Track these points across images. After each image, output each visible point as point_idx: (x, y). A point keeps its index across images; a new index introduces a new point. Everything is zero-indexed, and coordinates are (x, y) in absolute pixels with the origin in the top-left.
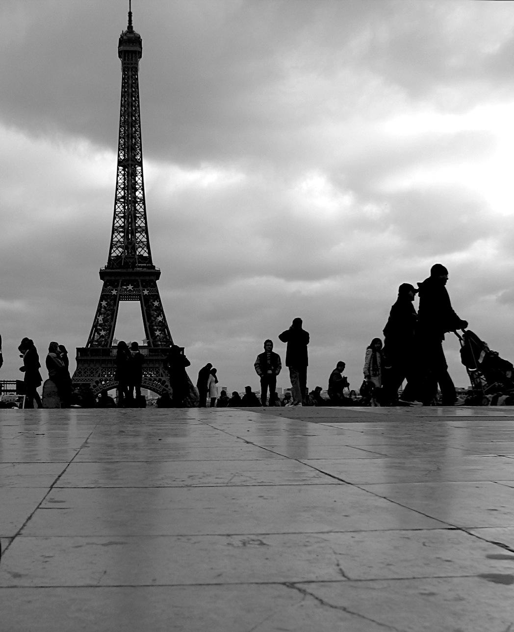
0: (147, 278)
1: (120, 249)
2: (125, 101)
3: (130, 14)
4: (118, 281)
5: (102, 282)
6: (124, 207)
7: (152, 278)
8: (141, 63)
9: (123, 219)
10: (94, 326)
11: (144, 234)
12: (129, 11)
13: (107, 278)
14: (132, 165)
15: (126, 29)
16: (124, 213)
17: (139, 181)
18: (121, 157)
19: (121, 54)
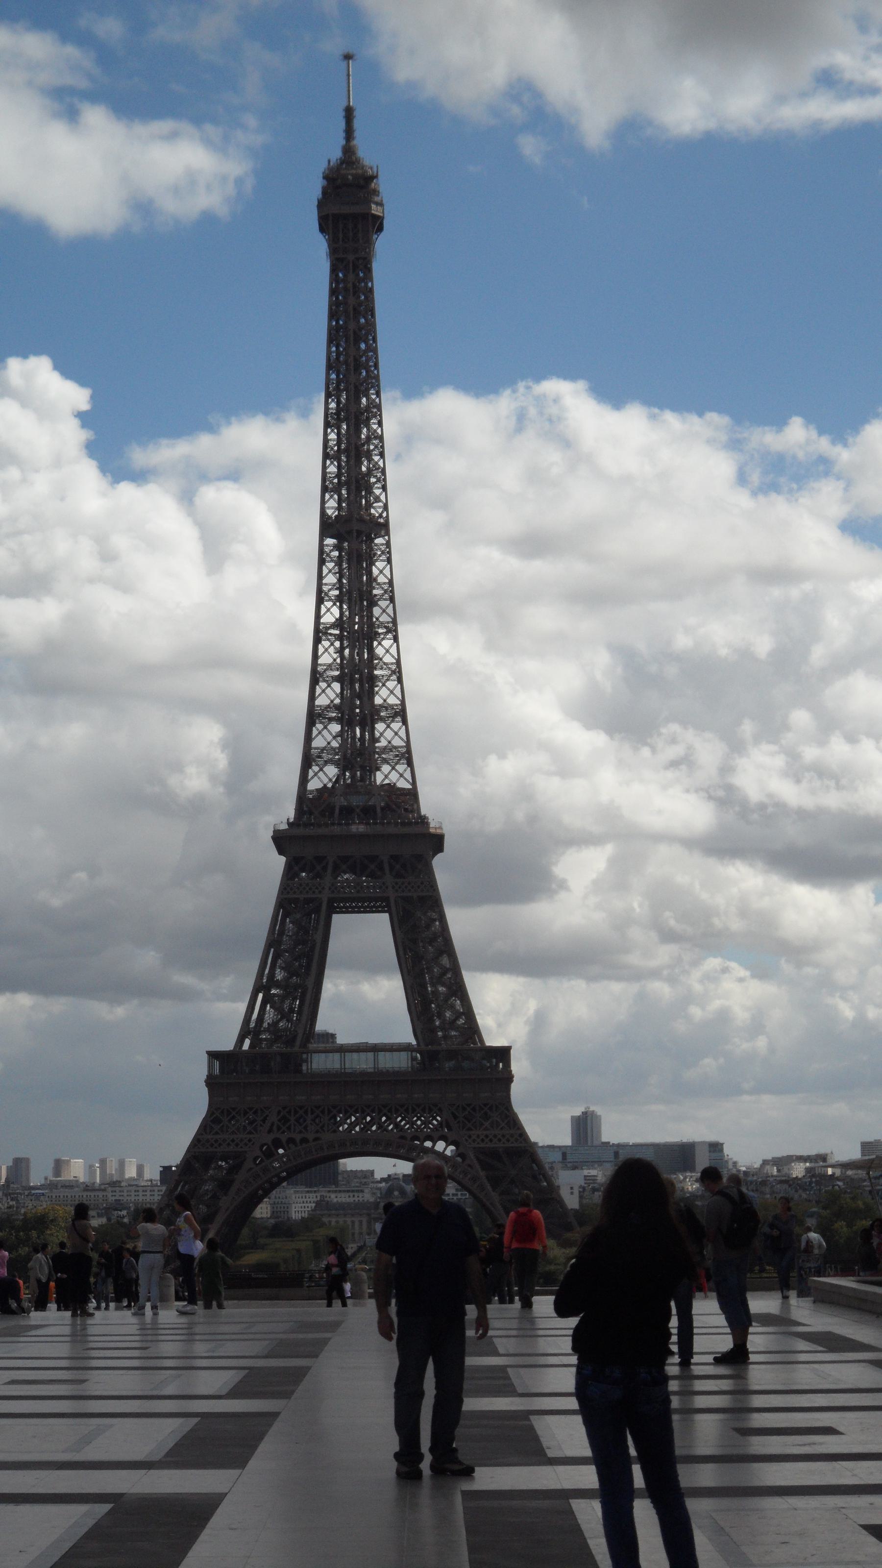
1: (332, 771)
2: (338, 354)
3: (349, 113)
5: (281, 861)
6: (340, 651)
9: (337, 686)
11: (396, 725)
12: (344, 104)
14: (359, 533)
15: (336, 154)
16: (342, 667)
17: (381, 579)
18: (329, 512)
19: (327, 223)
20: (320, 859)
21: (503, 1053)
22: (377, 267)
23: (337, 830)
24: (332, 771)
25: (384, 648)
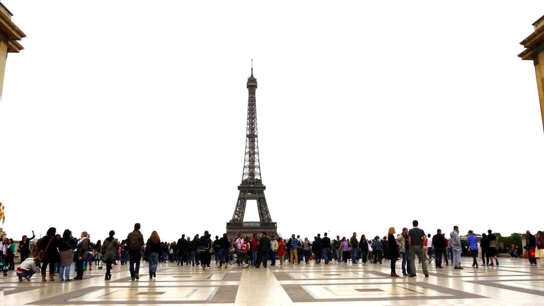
0: (260, 190)
1: (248, 176)
5: (239, 191)
10: (235, 212)
13: (241, 189)
15: (250, 76)
21: (276, 223)
23: (248, 186)
24: (248, 176)
25: (256, 156)
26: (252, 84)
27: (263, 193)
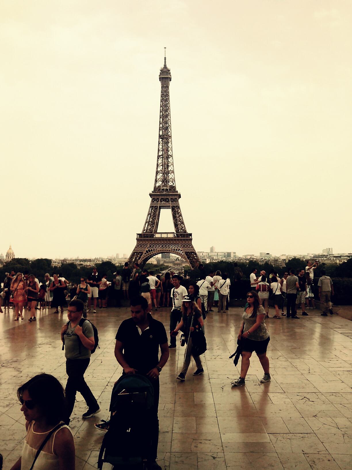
0: (173, 197)
1: (161, 183)
3: (165, 58)
4: (158, 199)
7: (176, 197)
8: (171, 83)
15: (163, 66)
19: (161, 79)
20: (158, 199)
21: (191, 235)
22: (170, 87)
26: (165, 77)
27: (177, 201)
